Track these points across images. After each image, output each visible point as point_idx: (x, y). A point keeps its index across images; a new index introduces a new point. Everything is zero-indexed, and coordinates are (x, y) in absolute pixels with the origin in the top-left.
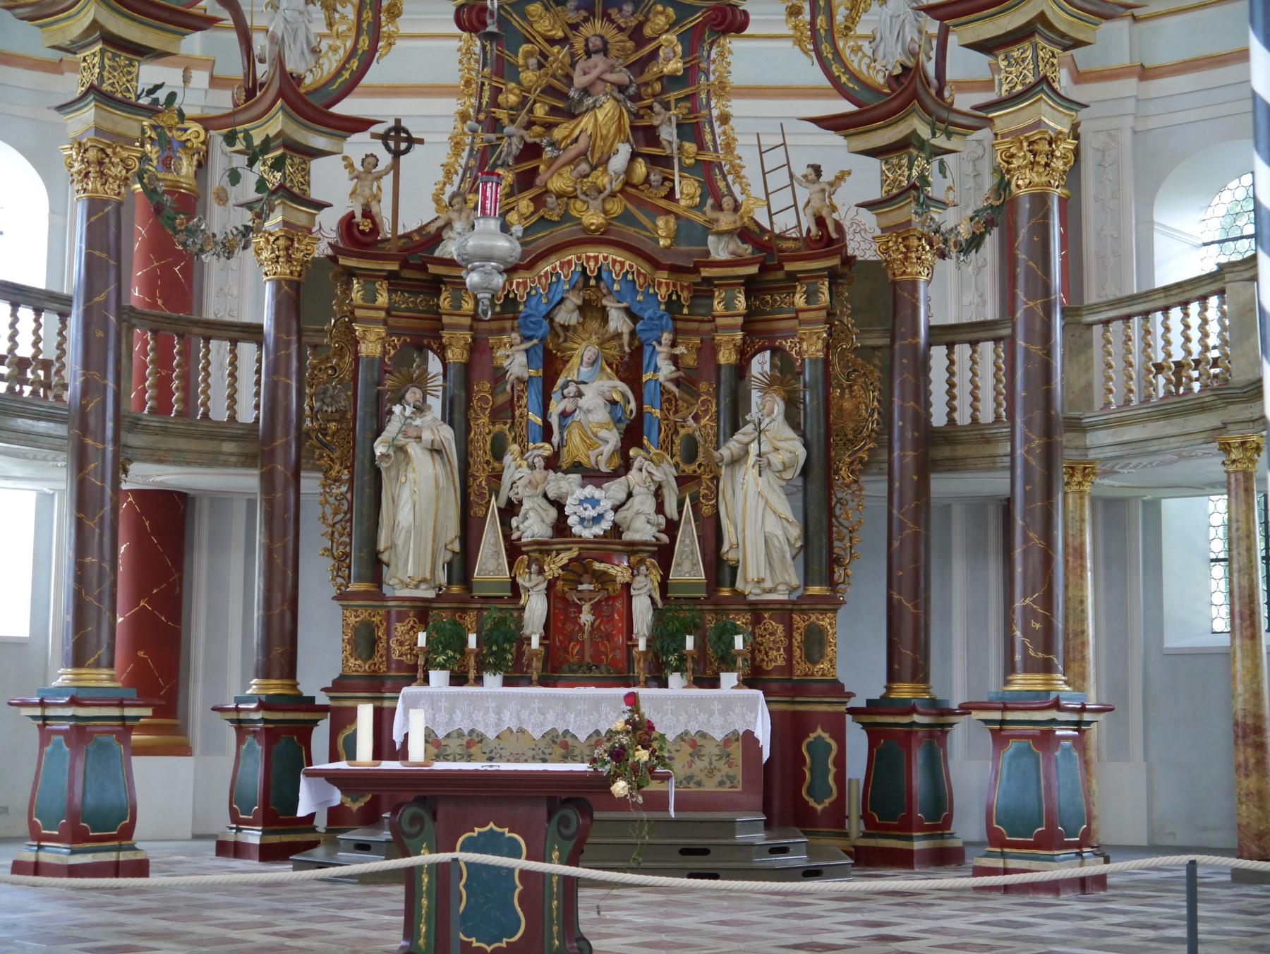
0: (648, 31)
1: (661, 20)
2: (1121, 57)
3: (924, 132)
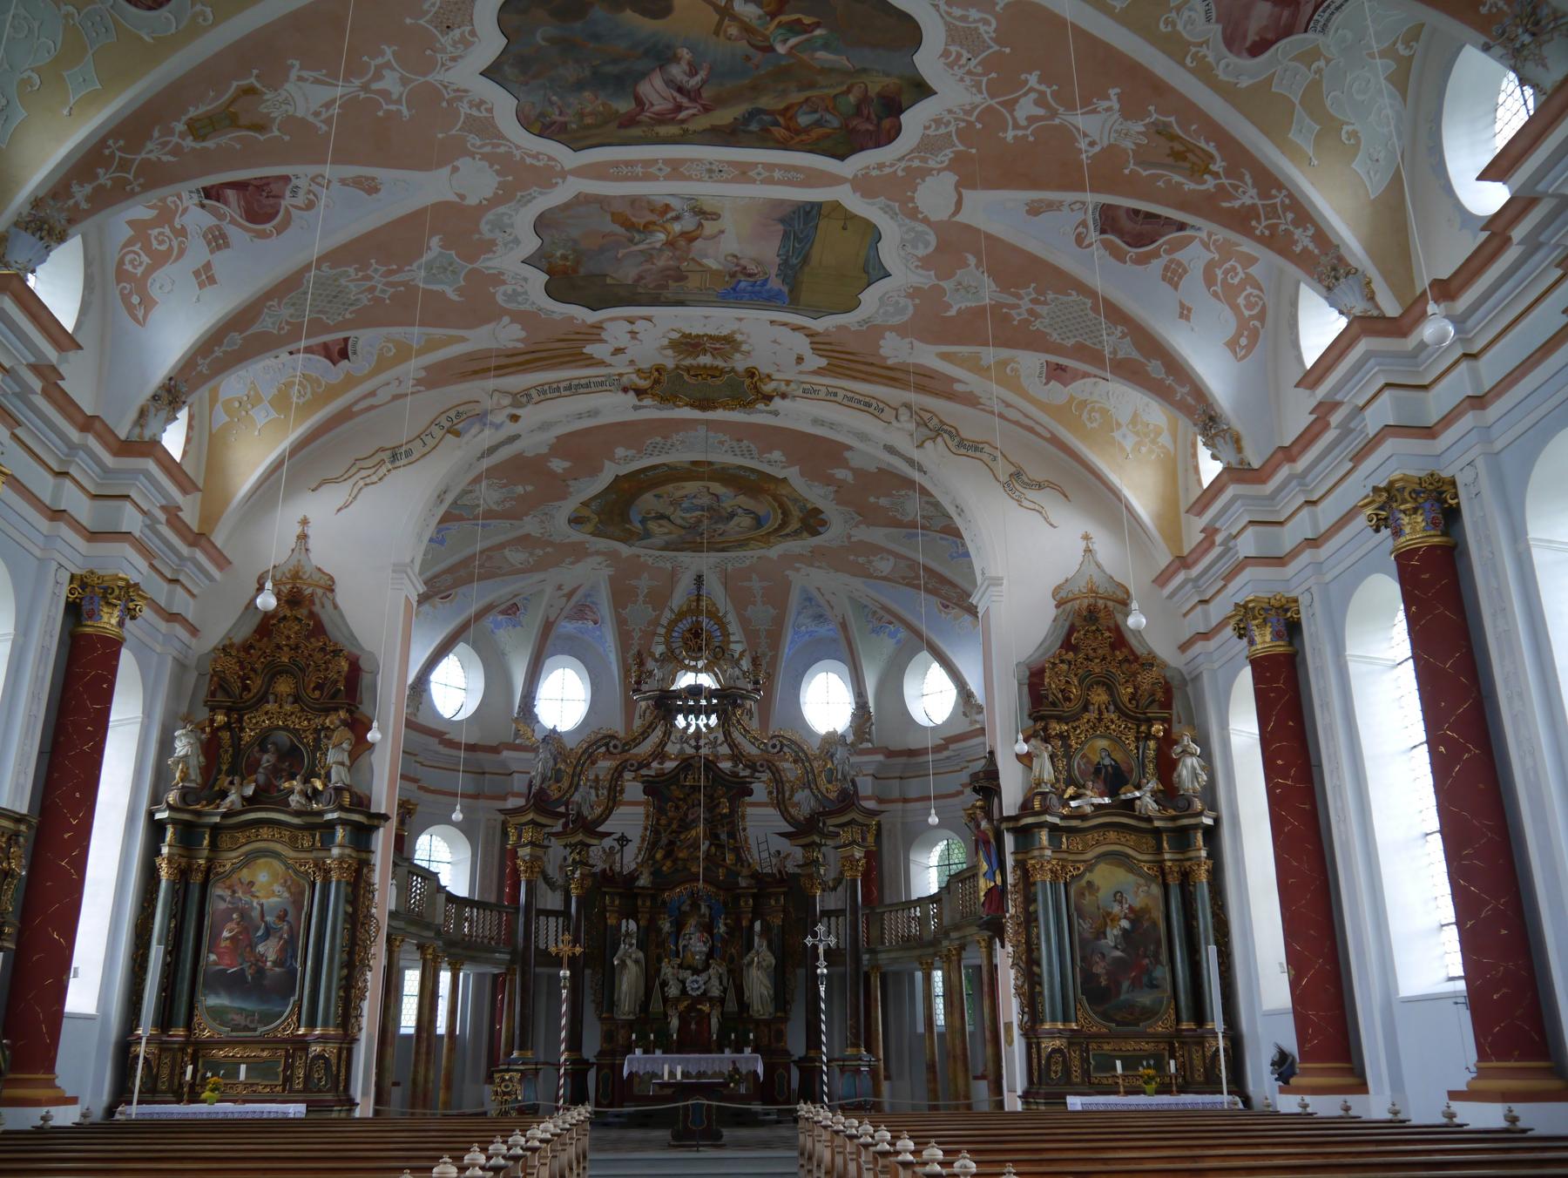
2: (896, 794)
3: (817, 840)
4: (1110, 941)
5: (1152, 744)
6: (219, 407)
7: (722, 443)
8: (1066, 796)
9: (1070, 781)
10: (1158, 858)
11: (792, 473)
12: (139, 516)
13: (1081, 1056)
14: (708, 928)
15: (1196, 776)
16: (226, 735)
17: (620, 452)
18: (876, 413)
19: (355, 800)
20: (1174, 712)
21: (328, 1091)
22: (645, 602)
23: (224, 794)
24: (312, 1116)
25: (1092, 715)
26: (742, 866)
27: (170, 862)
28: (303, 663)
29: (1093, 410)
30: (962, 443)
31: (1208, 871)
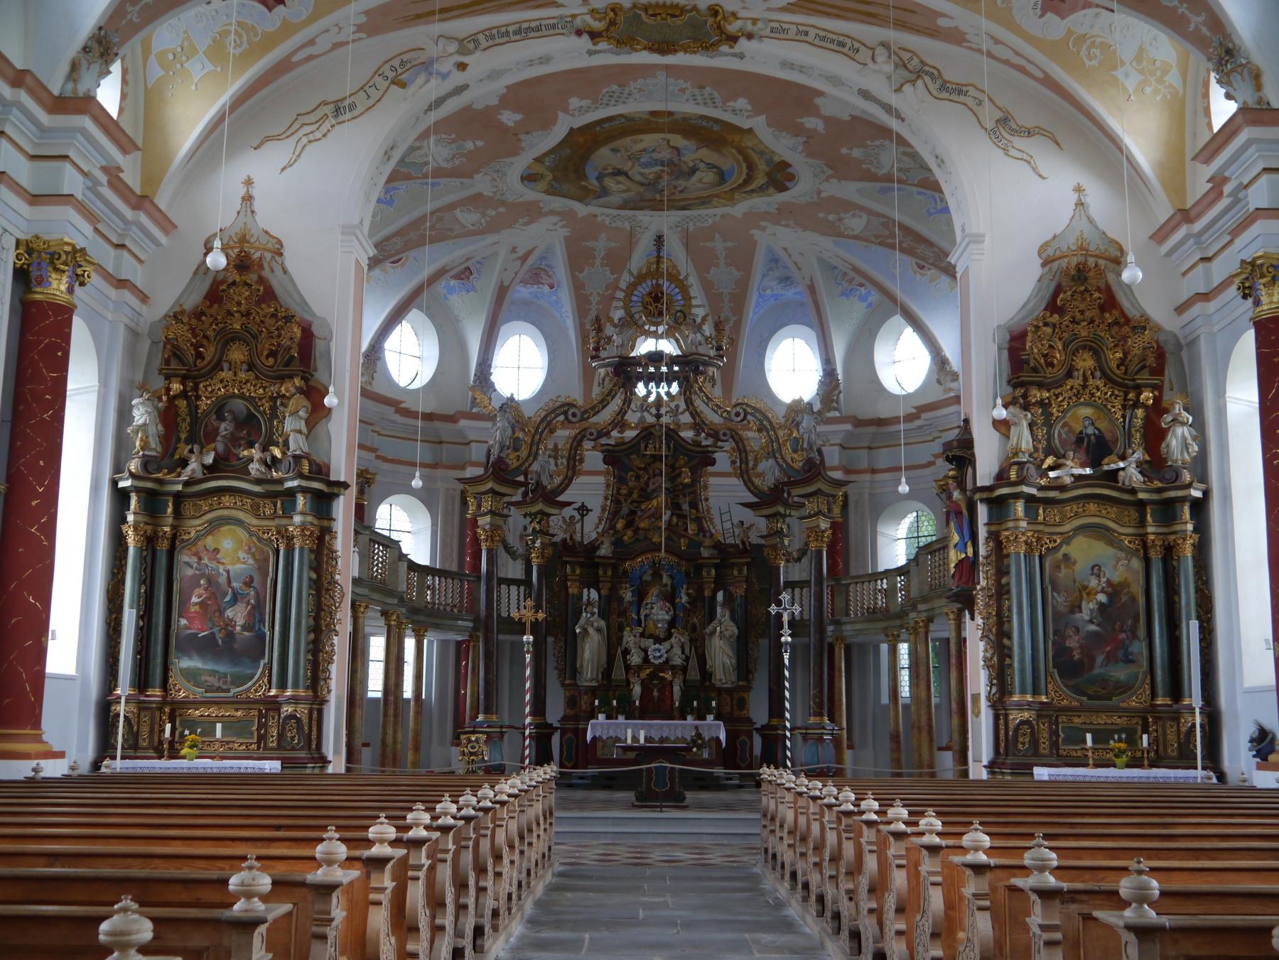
0: (677, 465)
1: (682, 462)
2: (864, 465)
3: (782, 510)
4: (1085, 615)
5: (1140, 412)
6: (152, 60)
7: (683, 91)
8: (1045, 466)
9: (1050, 451)
10: (1141, 531)
11: (758, 124)
12: (81, 178)
13: (1050, 727)
14: (670, 597)
15: (1186, 446)
16: (182, 404)
17: (574, 102)
18: (850, 53)
19: (314, 468)
20: (1166, 378)
21: (301, 749)
22: (602, 265)
23: (184, 463)
24: (287, 771)
25: (1077, 382)
26: (704, 536)
27: (136, 529)
28: (255, 329)
29: (1093, 45)
30: (944, 87)
31: (1193, 545)
